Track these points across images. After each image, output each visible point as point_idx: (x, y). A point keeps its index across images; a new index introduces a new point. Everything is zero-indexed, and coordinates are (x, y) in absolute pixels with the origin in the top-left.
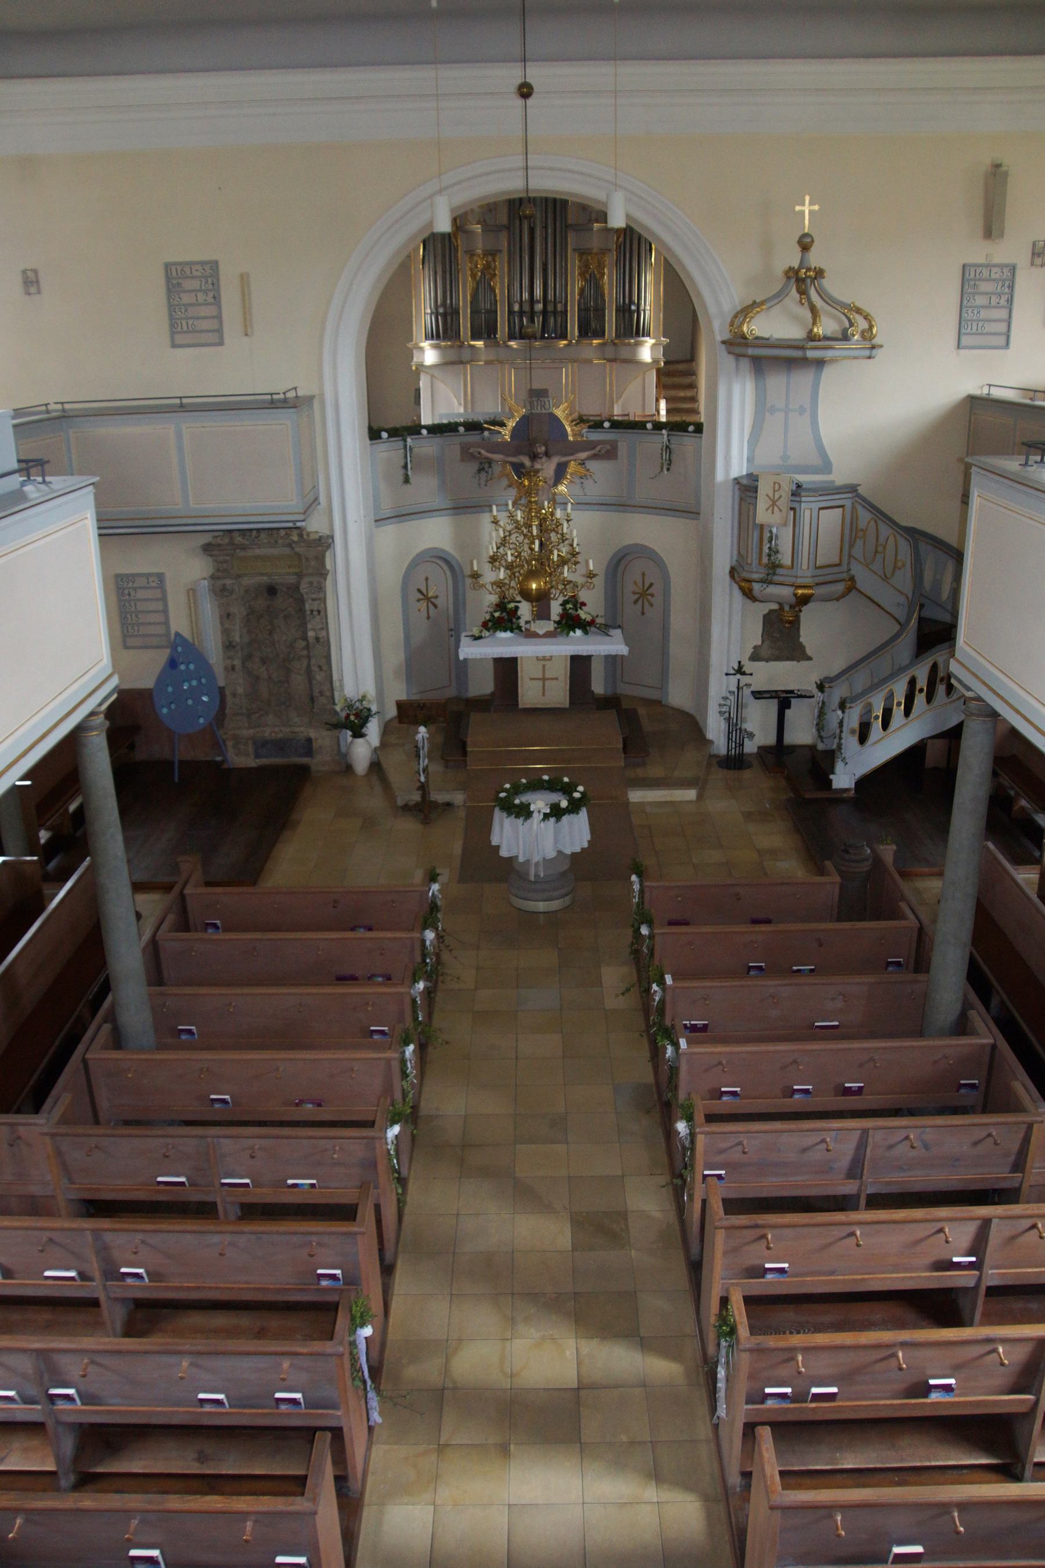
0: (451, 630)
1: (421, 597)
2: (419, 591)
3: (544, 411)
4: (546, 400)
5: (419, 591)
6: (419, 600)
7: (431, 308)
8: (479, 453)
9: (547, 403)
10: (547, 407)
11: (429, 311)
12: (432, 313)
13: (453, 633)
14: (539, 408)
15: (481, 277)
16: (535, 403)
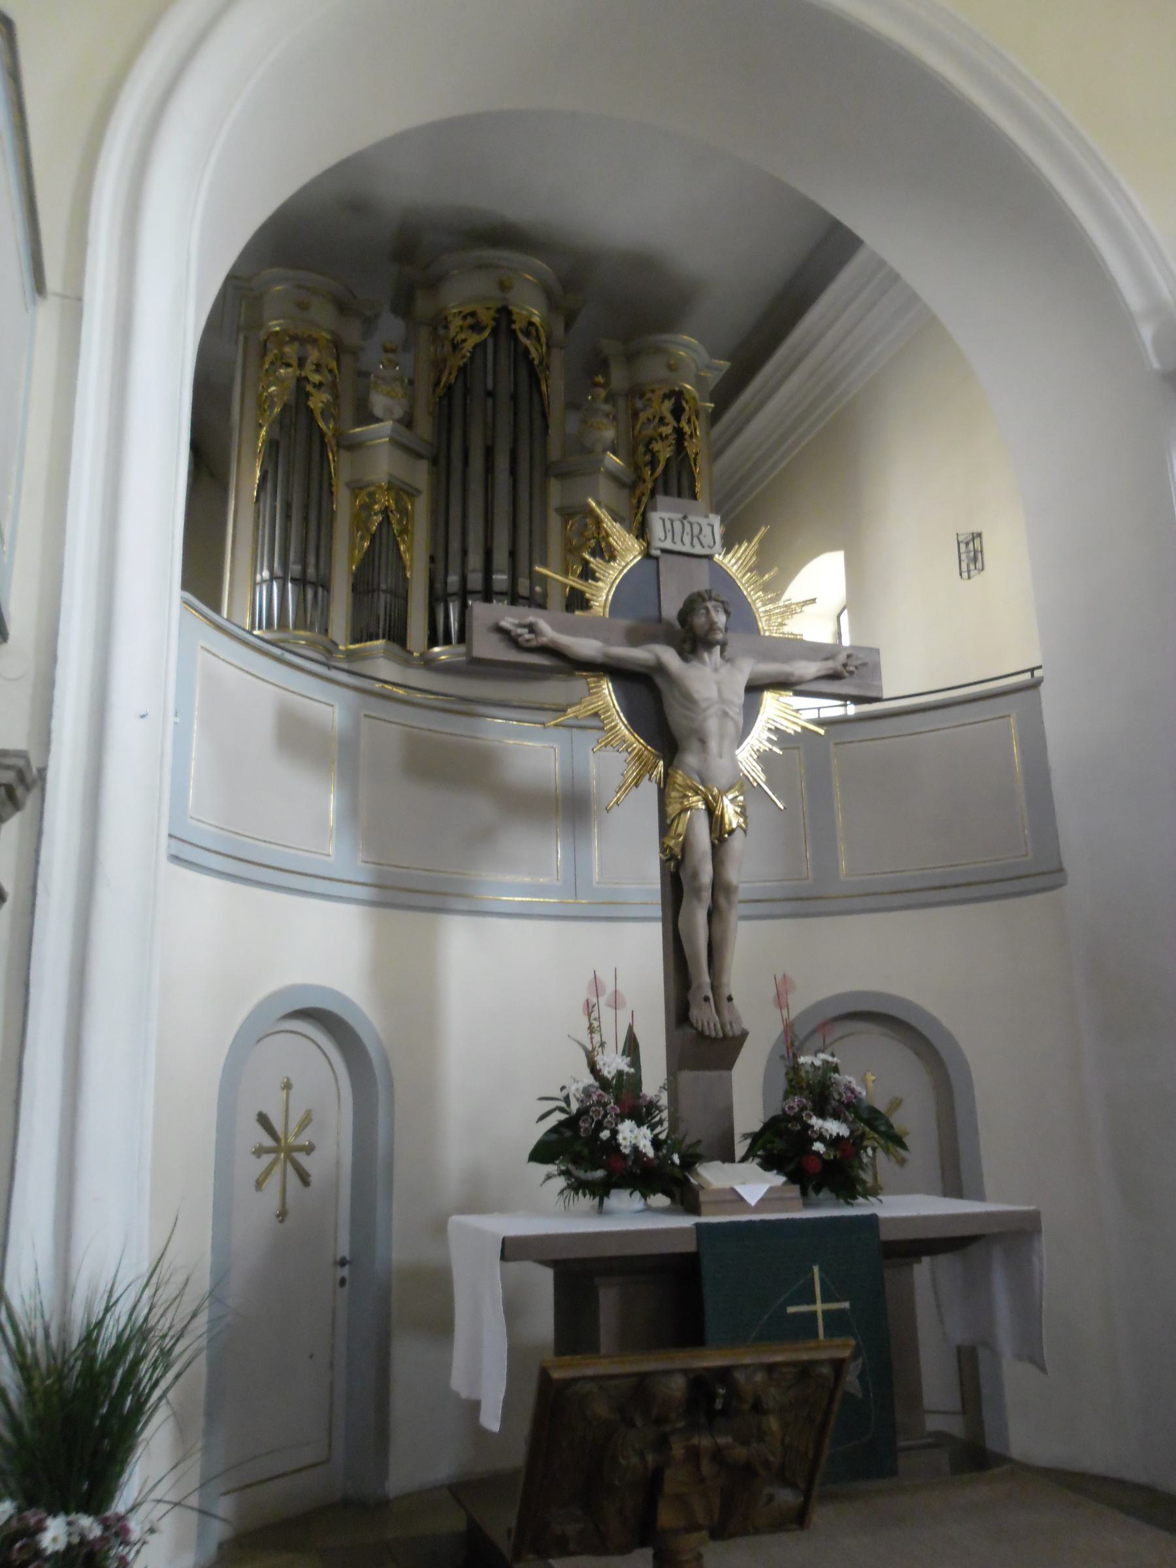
0: (343, 1263)
1: (268, 1142)
2: (264, 1121)
3: (698, 550)
4: (703, 522)
5: (264, 1121)
6: (259, 1151)
7: (271, 569)
8: (532, 628)
9: (707, 530)
10: (707, 540)
11: (266, 574)
12: (273, 577)
13: (345, 1272)
14: (687, 539)
15: (381, 524)
16: (677, 525)
